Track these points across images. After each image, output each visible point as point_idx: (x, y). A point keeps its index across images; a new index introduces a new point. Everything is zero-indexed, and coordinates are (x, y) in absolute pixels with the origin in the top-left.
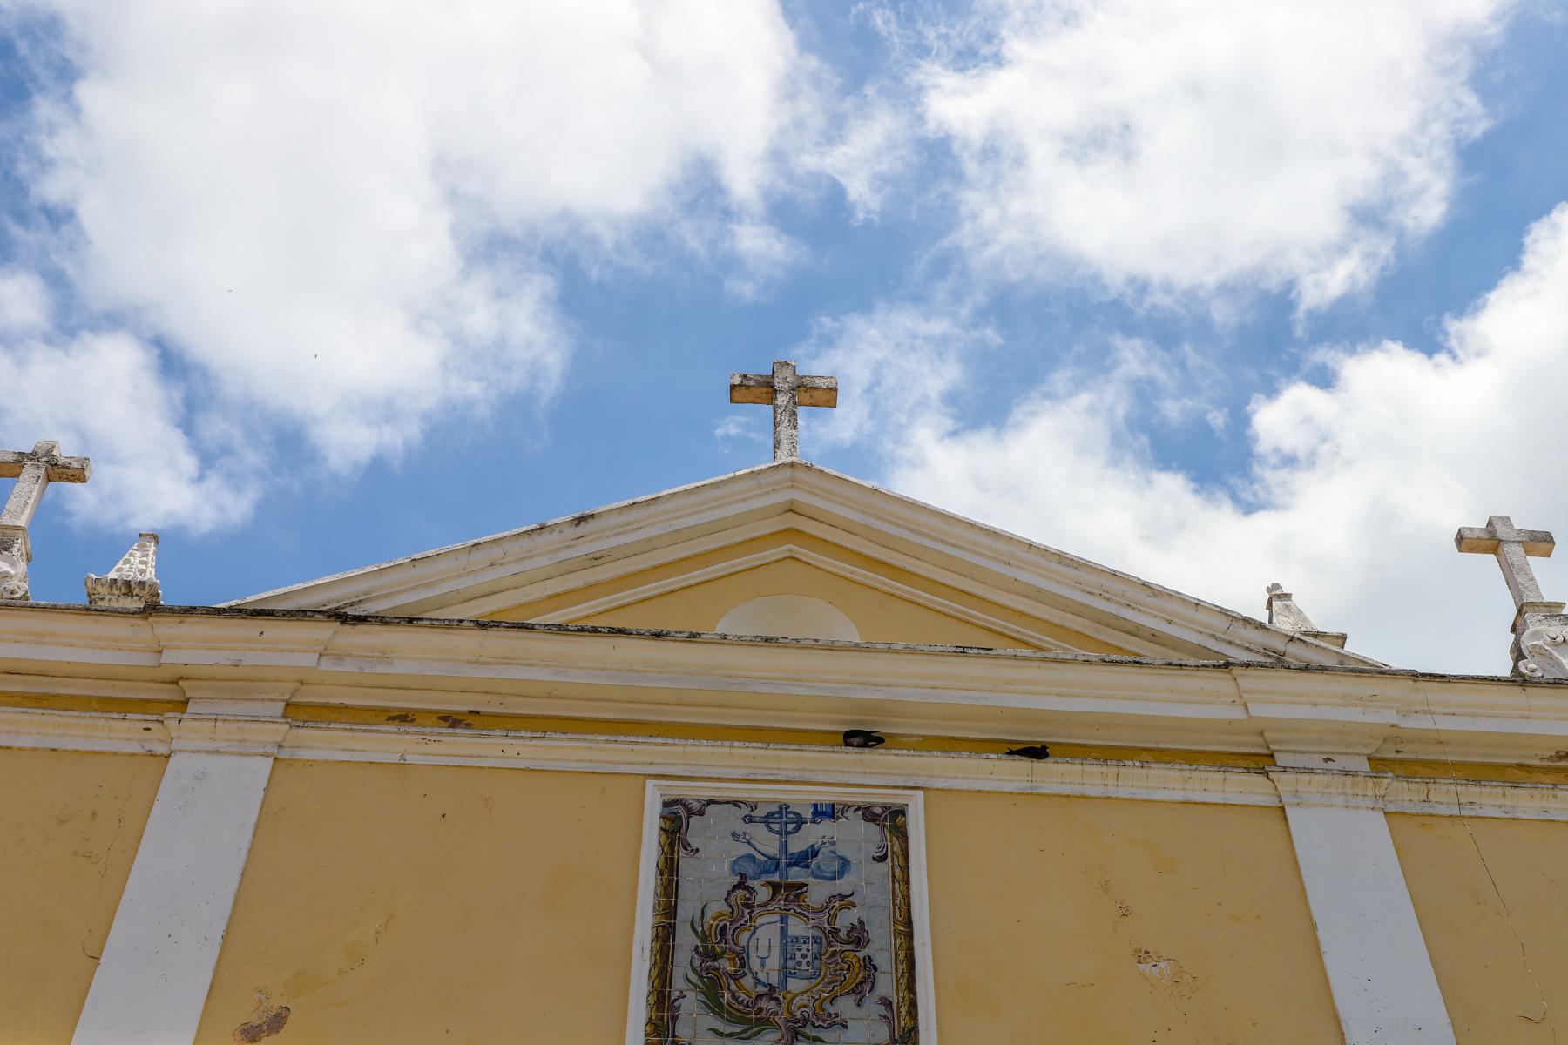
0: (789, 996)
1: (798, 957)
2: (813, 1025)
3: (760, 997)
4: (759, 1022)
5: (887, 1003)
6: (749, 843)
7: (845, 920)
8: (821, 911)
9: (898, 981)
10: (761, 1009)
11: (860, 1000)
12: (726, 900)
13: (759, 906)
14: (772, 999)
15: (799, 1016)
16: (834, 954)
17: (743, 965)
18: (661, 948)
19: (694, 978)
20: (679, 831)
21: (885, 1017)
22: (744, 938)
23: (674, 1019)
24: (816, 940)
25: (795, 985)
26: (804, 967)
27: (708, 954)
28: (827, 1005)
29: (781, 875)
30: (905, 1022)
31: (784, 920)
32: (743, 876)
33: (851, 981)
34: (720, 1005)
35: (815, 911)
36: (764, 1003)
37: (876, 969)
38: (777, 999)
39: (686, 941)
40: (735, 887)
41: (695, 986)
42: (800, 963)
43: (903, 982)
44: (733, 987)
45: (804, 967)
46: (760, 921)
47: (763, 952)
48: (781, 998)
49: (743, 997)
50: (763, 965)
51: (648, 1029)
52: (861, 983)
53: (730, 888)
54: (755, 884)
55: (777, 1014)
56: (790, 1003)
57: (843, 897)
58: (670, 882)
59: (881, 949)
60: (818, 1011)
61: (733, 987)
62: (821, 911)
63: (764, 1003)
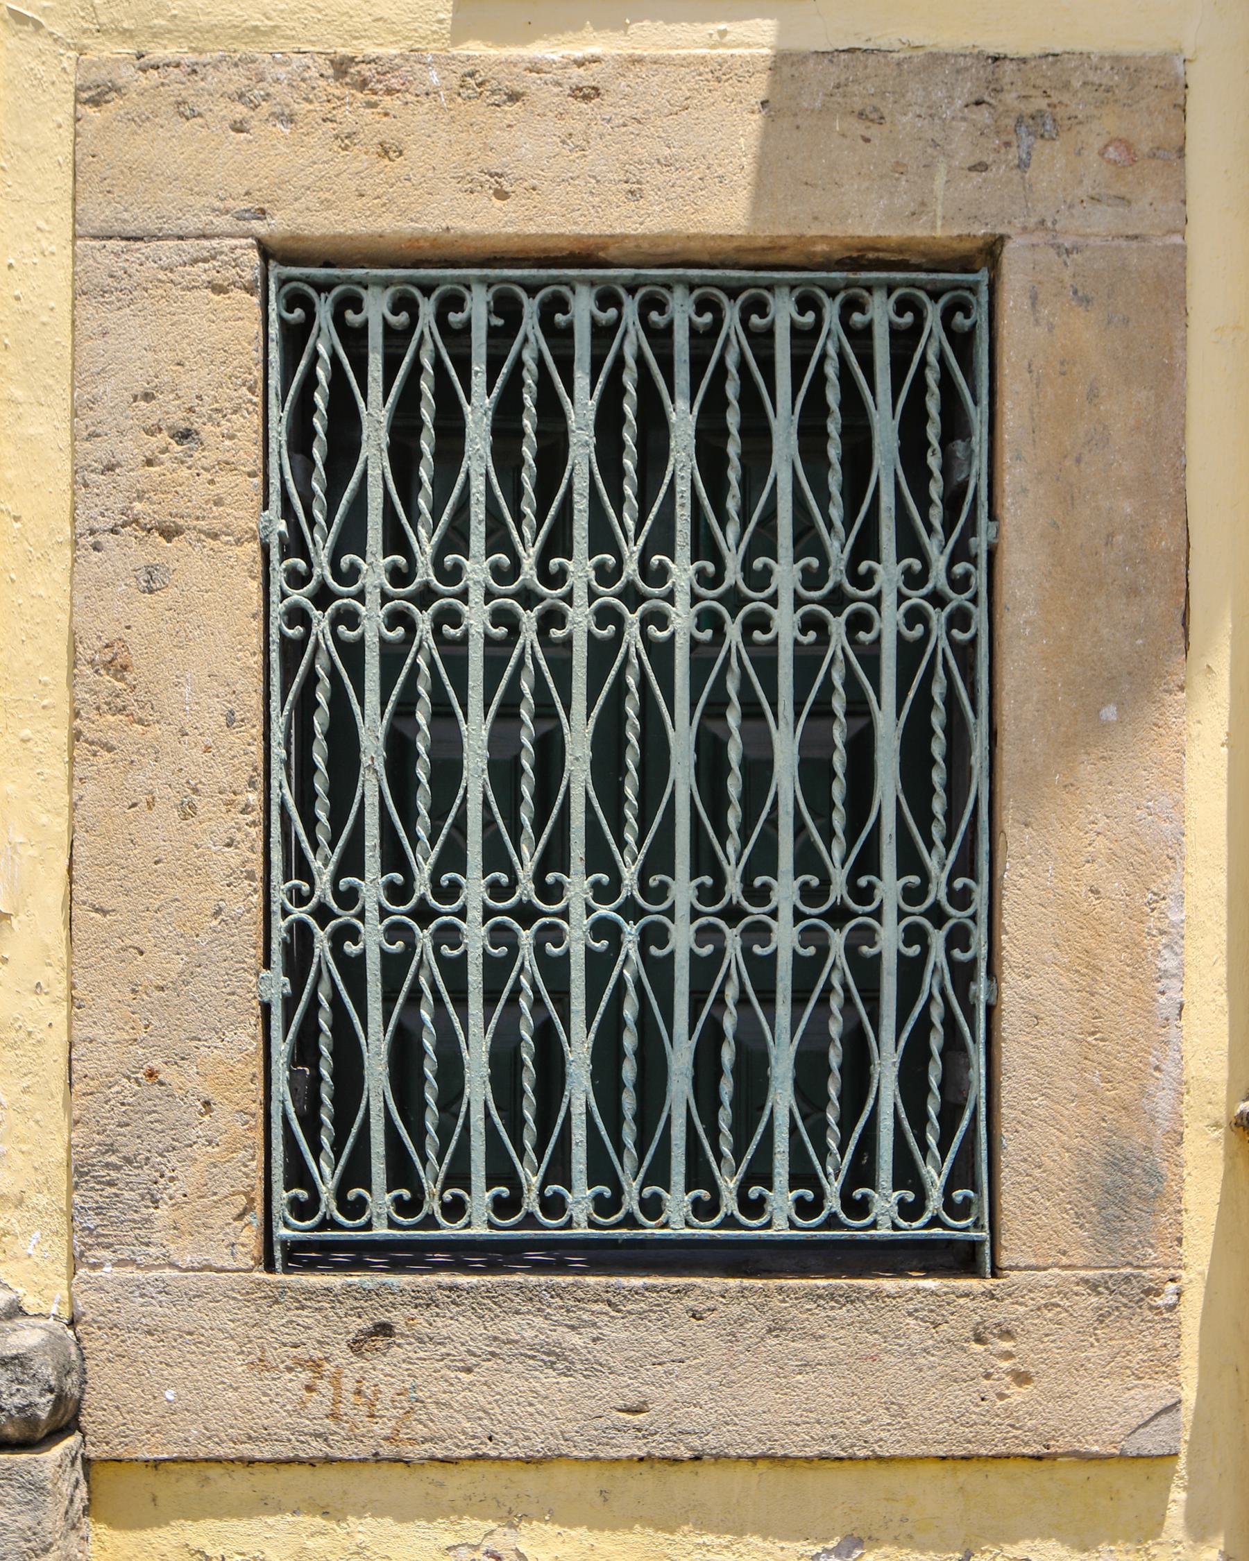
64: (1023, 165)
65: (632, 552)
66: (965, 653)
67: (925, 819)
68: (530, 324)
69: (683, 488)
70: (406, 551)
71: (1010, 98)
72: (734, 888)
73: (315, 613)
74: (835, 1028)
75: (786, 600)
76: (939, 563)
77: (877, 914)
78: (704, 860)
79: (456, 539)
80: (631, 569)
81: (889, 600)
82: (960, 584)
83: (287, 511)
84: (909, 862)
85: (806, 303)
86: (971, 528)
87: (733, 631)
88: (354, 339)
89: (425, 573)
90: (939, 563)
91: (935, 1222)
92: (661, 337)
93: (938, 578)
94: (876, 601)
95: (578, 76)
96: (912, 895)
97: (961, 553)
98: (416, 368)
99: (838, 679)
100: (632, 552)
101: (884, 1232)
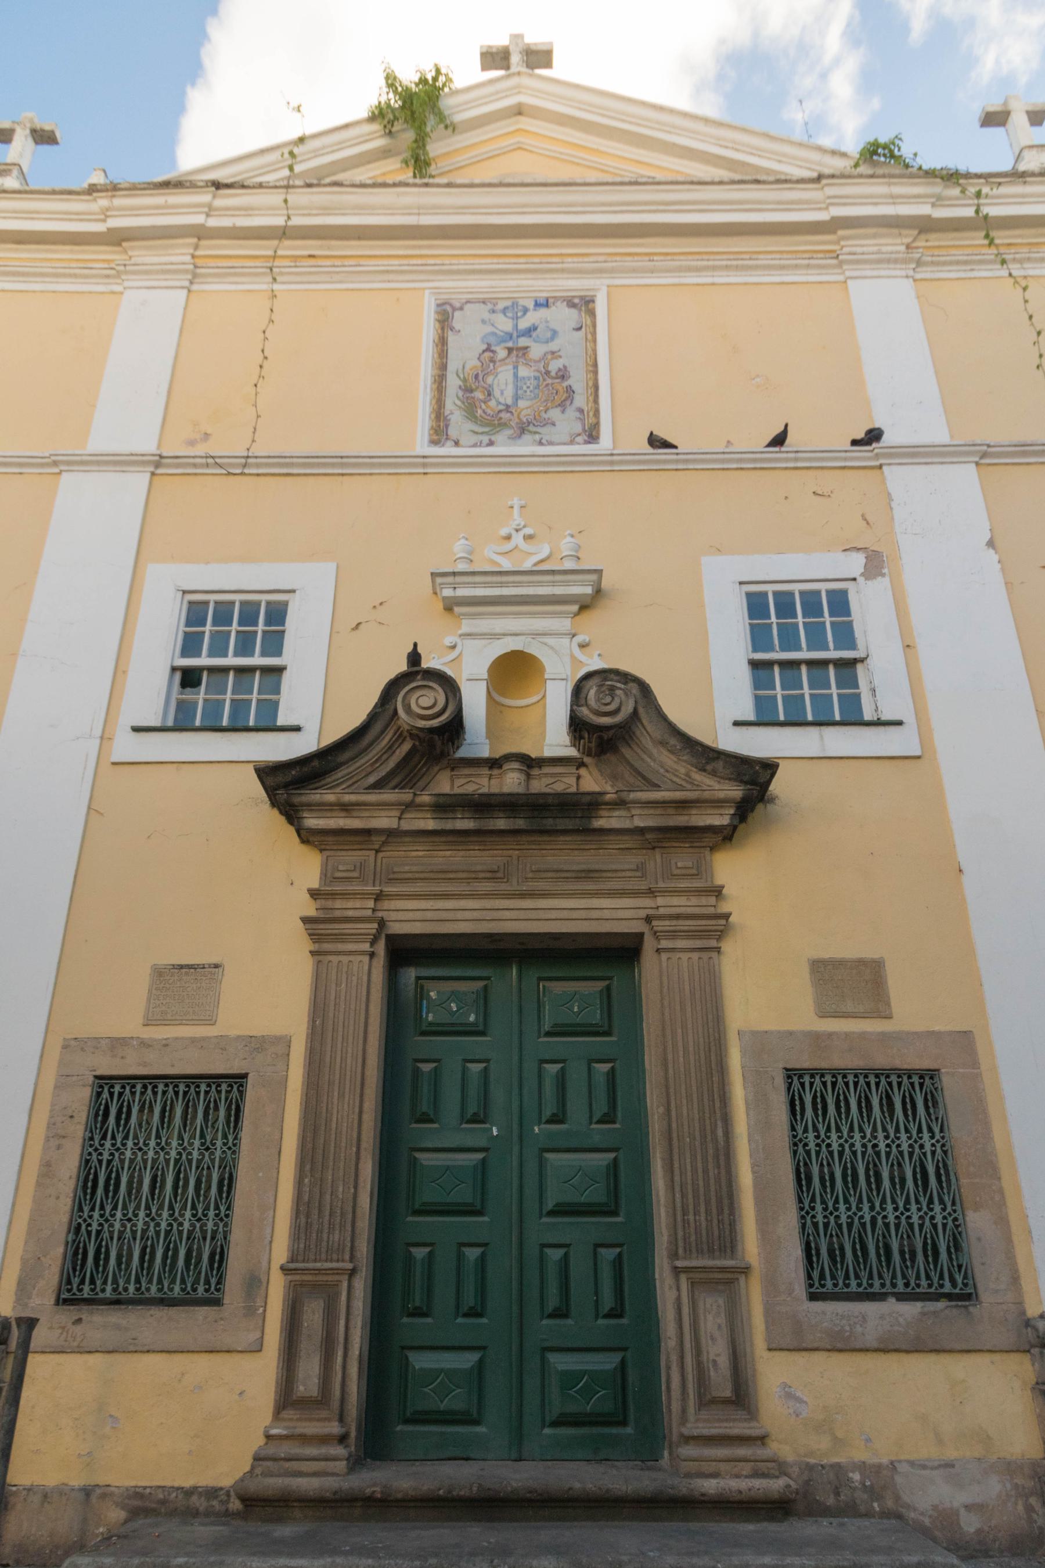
0: (519, 410)
1: (525, 388)
2: (534, 425)
3: (500, 411)
4: (500, 425)
5: (581, 411)
6: (493, 325)
7: (554, 366)
8: (539, 361)
9: (588, 398)
10: (501, 418)
11: (564, 410)
12: (479, 359)
13: (500, 361)
14: (508, 412)
15: (525, 420)
16: (547, 385)
17: (489, 395)
18: (438, 387)
19: (458, 403)
20: (448, 318)
21: (580, 419)
22: (490, 379)
23: (447, 426)
24: (536, 378)
25: (522, 404)
26: (528, 393)
27: (468, 390)
28: (543, 415)
29: (514, 342)
30: (592, 420)
31: (516, 368)
32: (489, 345)
33: (558, 399)
34: (476, 417)
35: (535, 361)
36: (503, 415)
37: (574, 392)
38: (511, 412)
39: (453, 383)
40: (484, 351)
41: (460, 407)
42: (526, 392)
43: (591, 399)
44: (484, 406)
45: (528, 393)
46: (499, 369)
47: (503, 387)
48: (514, 411)
49: (489, 411)
50: (502, 393)
51: (431, 432)
52: (564, 400)
53: (481, 351)
54: (498, 349)
55: (511, 420)
56: (520, 413)
57: (553, 353)
58: (443, 351)
59: (578, 380)
60: (537, 417)
61: (484, 406)
62: (539, 361)
63: (503, 415)
64: (253, 1058)
65: (164, 1139)
66: (234, 1160)
67: (221, 1198)
68: (149, 1091)
69: (177, 1125)
70: (115, 1140)
71: (253, 1045)
72: (176, 1214)
73: (93, 1153)
74: (195, 1247)
75: (196, 1149)
76: (231, 1140)
77: (208, 1220)
78: (171, 1208)
79: (126, 1137)
80: (163, 1143)
81: (219, 1149)
82: (235, 1145)
83: (91, 1131)
84: (217, 1208)
85: (209, 1085)
86: (237, 1134)
87: (184, 1156)
88: (111, 1094)
89: (119, 1145)
90: (231, 1140)
91: (212, 1293)
92: (176, 1093)
93: (230, 1144)
94: (216, 1149)
95: (164, 1042)
96: (217, 1215)
97: (236, 1138)
98: (124, 1101)
99: (205, 1166)
100: (164, 1139)
101: (200, 1295)
